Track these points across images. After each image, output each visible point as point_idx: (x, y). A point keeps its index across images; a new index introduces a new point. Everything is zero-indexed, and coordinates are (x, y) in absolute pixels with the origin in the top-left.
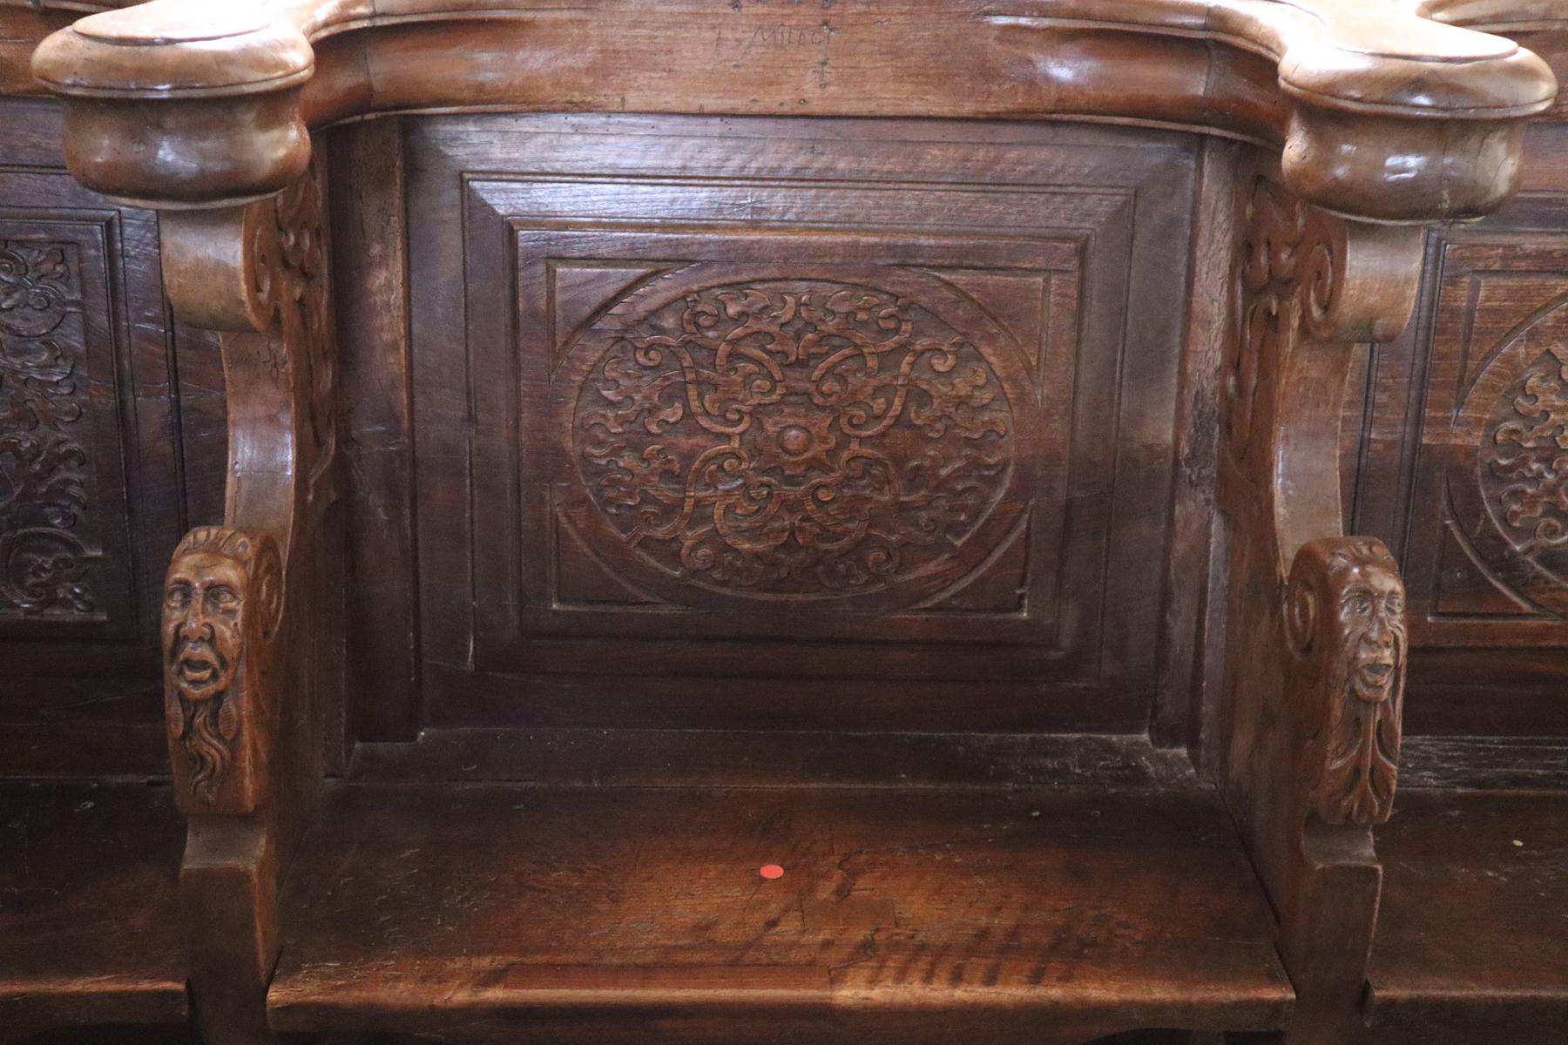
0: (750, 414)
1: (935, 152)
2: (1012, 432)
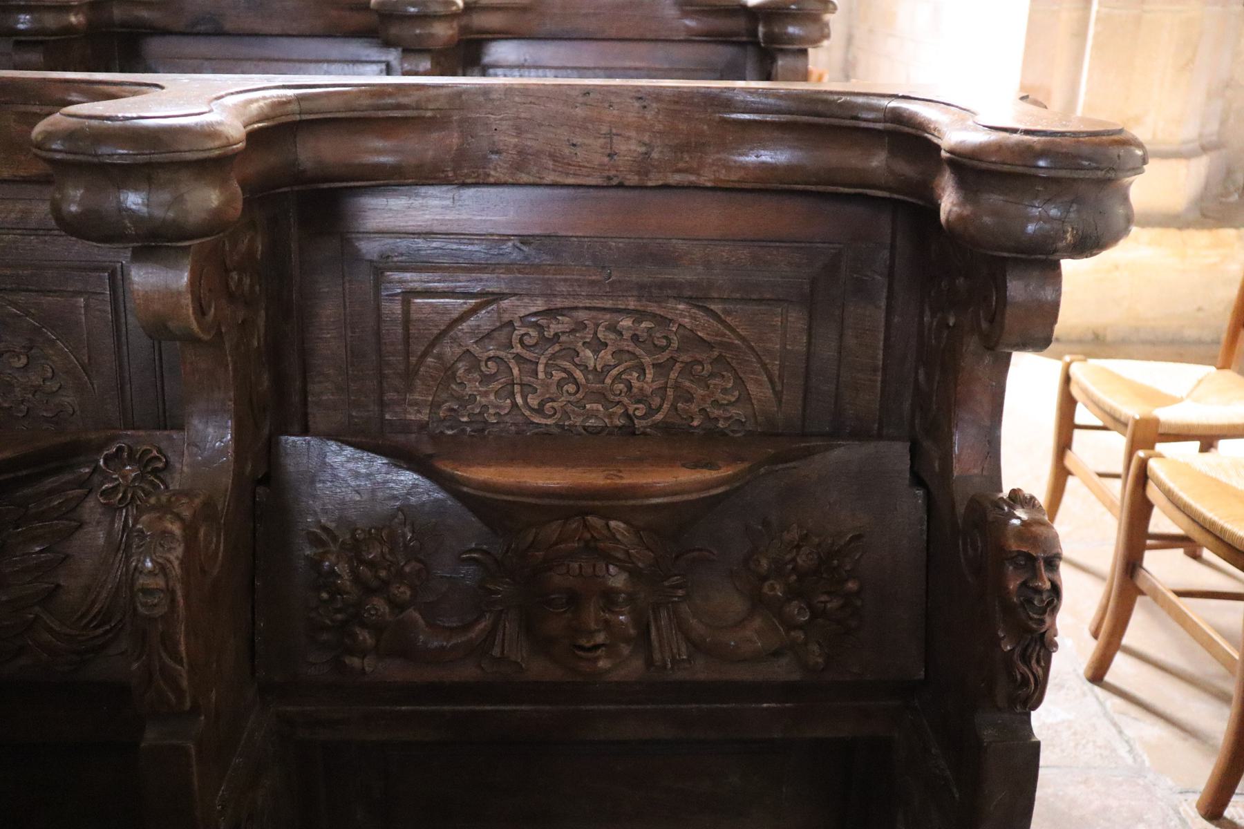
2: (78, 413)
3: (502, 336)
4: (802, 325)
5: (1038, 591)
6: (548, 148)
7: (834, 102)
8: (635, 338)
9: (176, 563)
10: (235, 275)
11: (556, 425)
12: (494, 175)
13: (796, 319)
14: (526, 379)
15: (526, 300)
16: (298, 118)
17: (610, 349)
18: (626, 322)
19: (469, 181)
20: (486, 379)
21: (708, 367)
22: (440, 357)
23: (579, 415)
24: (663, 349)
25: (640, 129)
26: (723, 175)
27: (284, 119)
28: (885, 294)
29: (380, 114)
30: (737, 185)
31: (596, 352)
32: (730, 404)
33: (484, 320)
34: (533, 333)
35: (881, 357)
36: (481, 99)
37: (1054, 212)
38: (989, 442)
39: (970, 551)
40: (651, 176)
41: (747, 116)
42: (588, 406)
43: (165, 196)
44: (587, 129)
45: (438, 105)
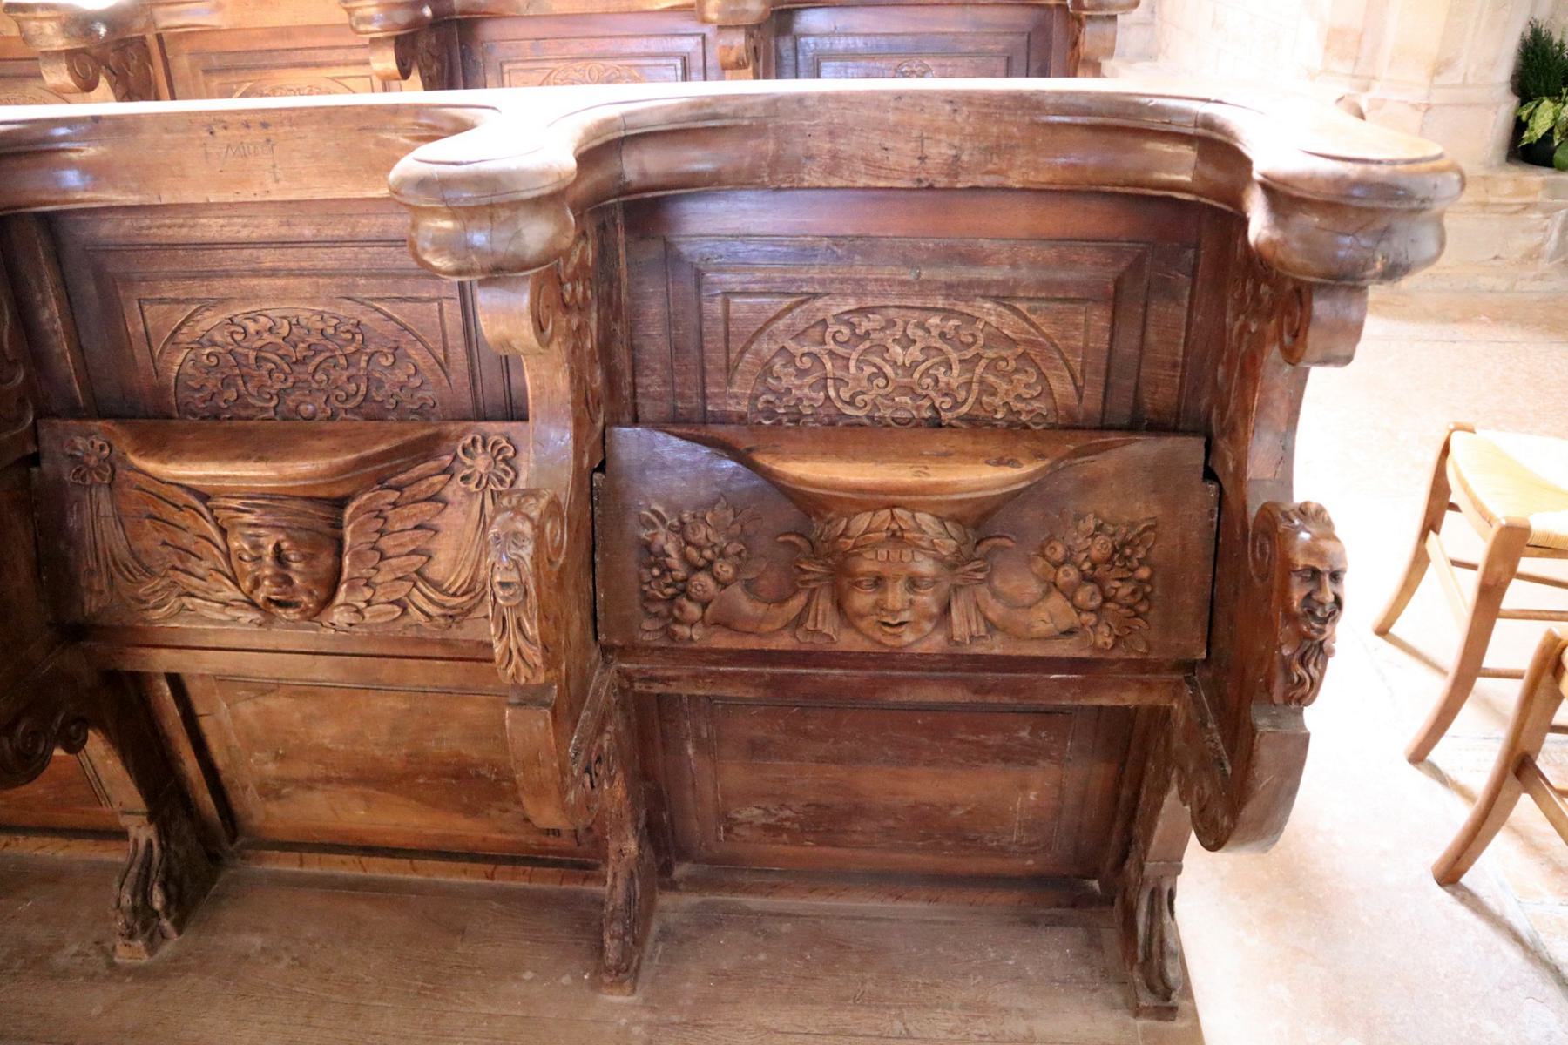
0: (277, 395)
1: (364, 221)
3: (817, 331)
4: (1105, 324)
5: (1322, 604)
6: (860, 153)
7: (1145, 105)
8: (942, 335)
9: (527, 559)
10: (569, 287)
11: (868, 417)
12: (809, 180)
13: (1099, 318)
14: (839, 374)
15: (839, 299)
16: (623, 134)
17: (919, 345)
18: (934, 320)
19: (784, 186)
20: (802, 373)
21: (1012, 364)
22: (757, 353)
23: (888, 407)
24: (969, 346)
25: (950, 133)
26: (1032, 176)
27: (610, 137)
28: (1187, 293)
29: (700, 124)
30: (1045, 187)
31: (905, 348)
32: (1033, 398)
33: (799, 318)
34: (846, 330)
35: (1181, 353)
36: (795, 106)
37: (1364, 242)
38: (1284, 448)
39: (1258, 555)
40: (961, 178)
41: (1057, 119)
42: (897, 399)
43: (505, 234)
44: (898, 132)
45: (755, 114)
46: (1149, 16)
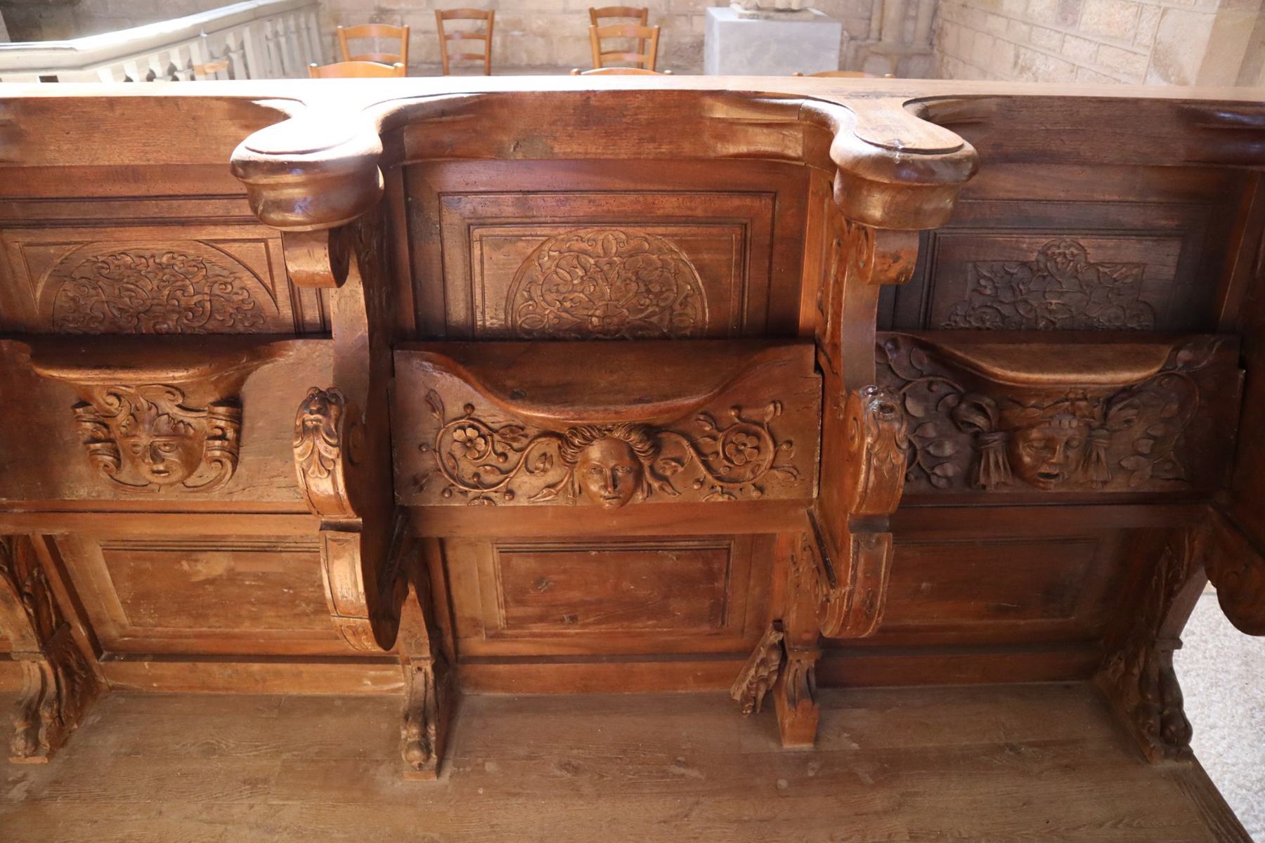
46: (928, 48)
